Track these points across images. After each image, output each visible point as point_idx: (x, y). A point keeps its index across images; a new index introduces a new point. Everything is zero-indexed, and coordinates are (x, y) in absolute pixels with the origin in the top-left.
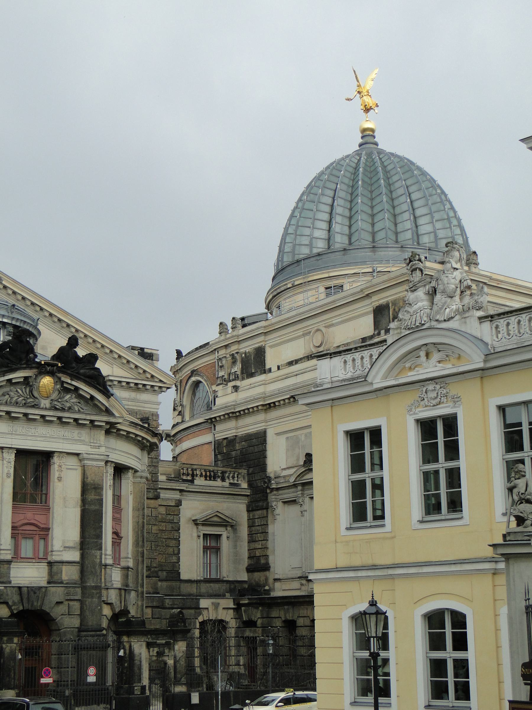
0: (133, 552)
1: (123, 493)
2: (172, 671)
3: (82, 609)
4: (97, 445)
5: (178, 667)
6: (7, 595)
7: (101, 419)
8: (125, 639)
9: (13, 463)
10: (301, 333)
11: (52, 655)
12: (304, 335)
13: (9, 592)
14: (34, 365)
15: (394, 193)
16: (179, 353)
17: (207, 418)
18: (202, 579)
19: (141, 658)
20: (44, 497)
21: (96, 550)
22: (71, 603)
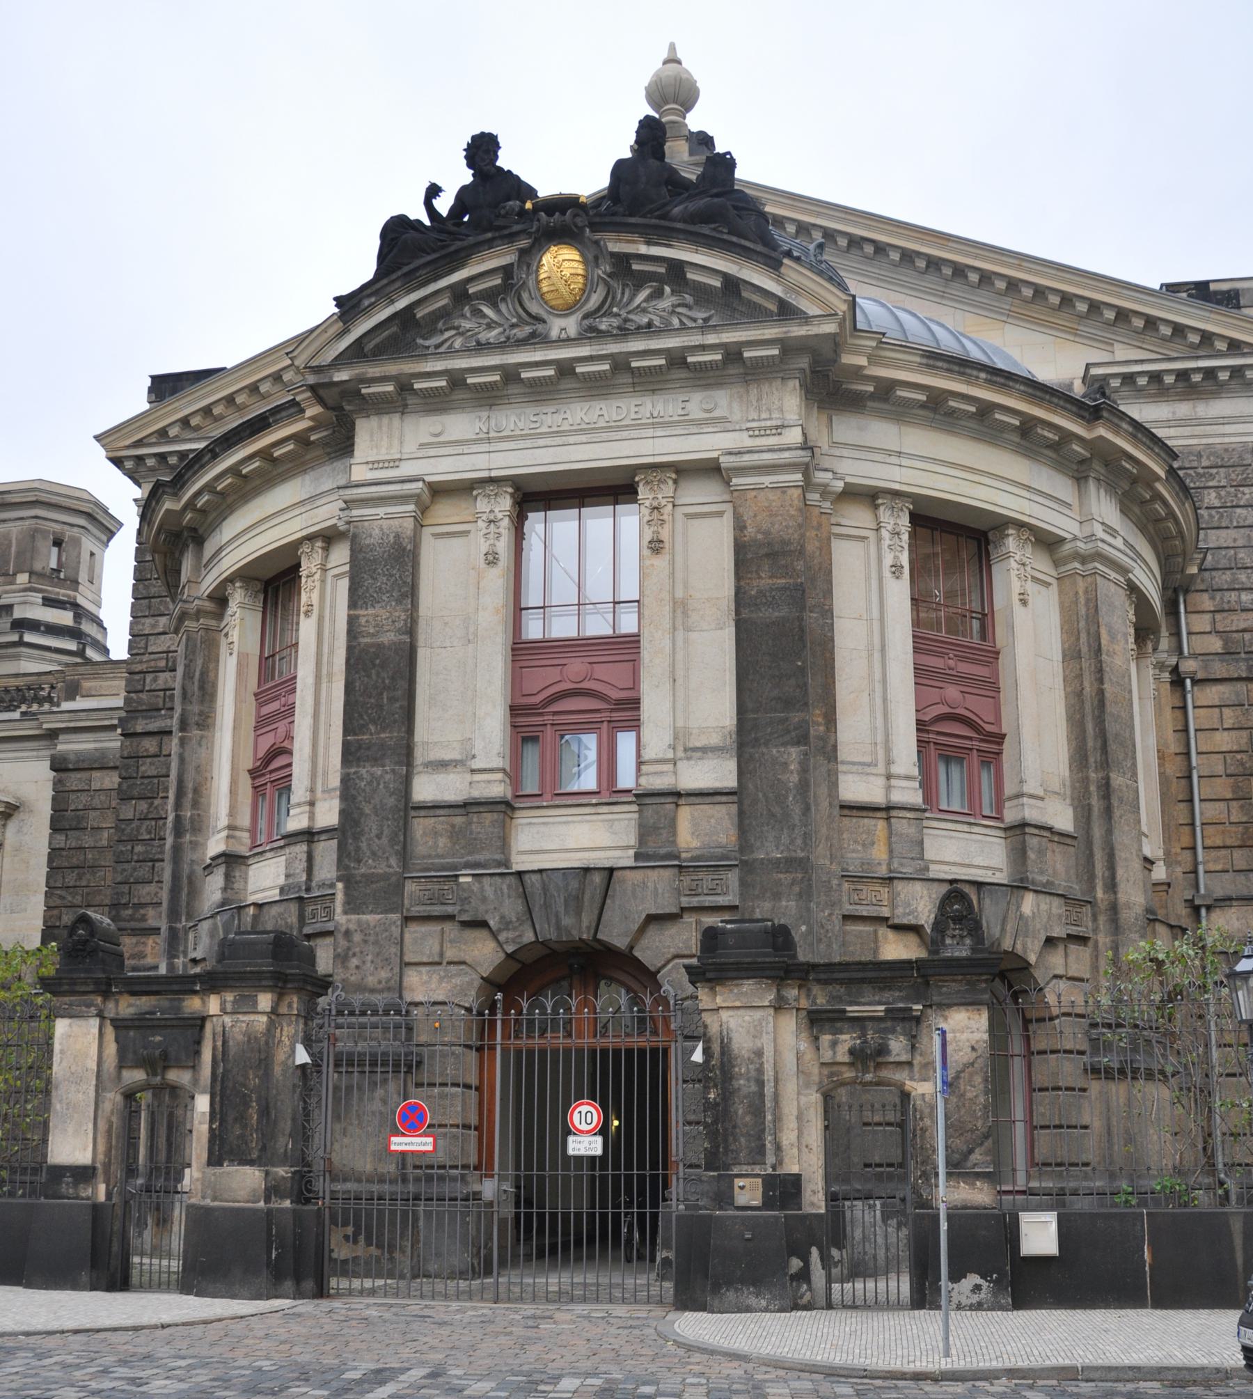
4: (769, 423)
6: (484, 900)
13: (489, 892)
19: (760, 1071)
21: (784, 744)
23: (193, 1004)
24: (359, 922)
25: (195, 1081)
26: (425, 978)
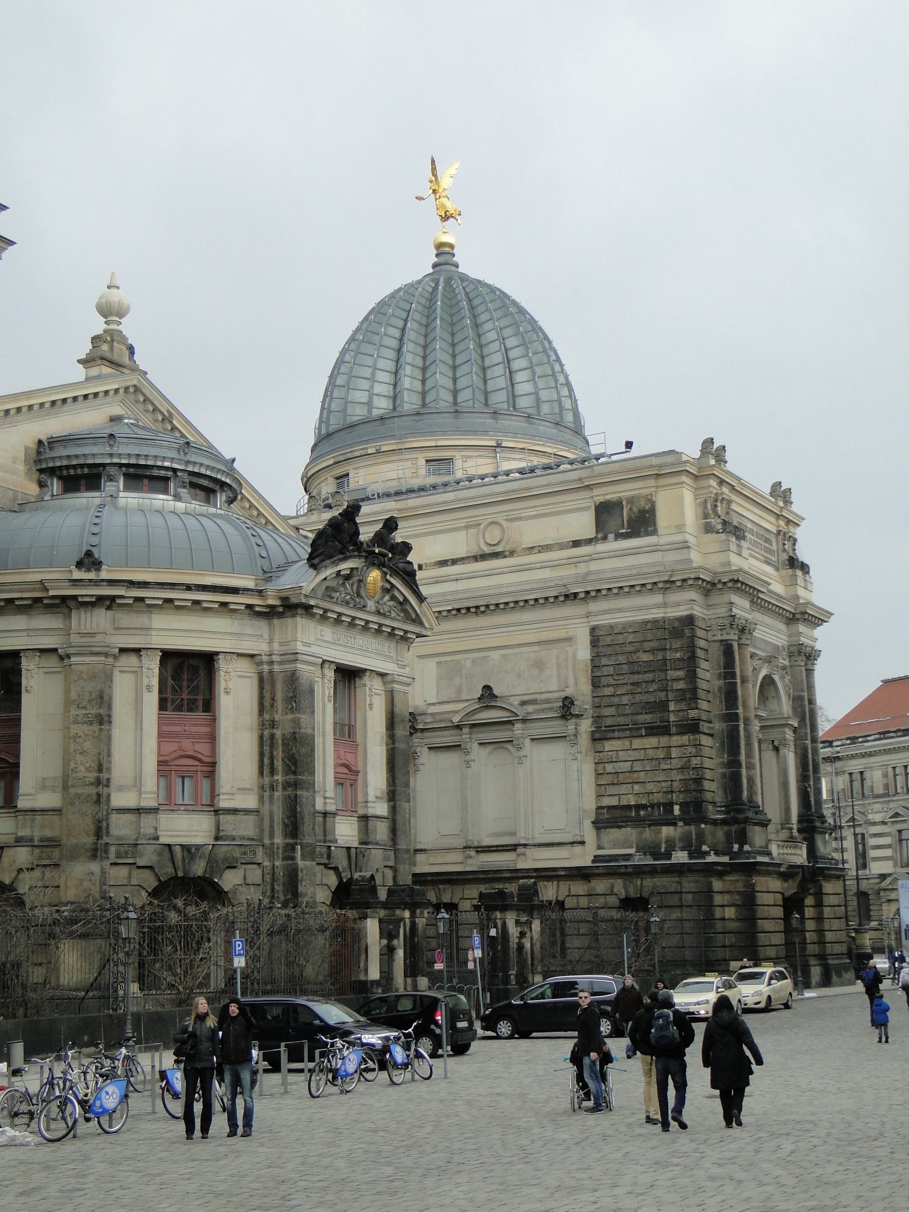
10: (463, 524)
12: (467, 527)
15: (483, 338)
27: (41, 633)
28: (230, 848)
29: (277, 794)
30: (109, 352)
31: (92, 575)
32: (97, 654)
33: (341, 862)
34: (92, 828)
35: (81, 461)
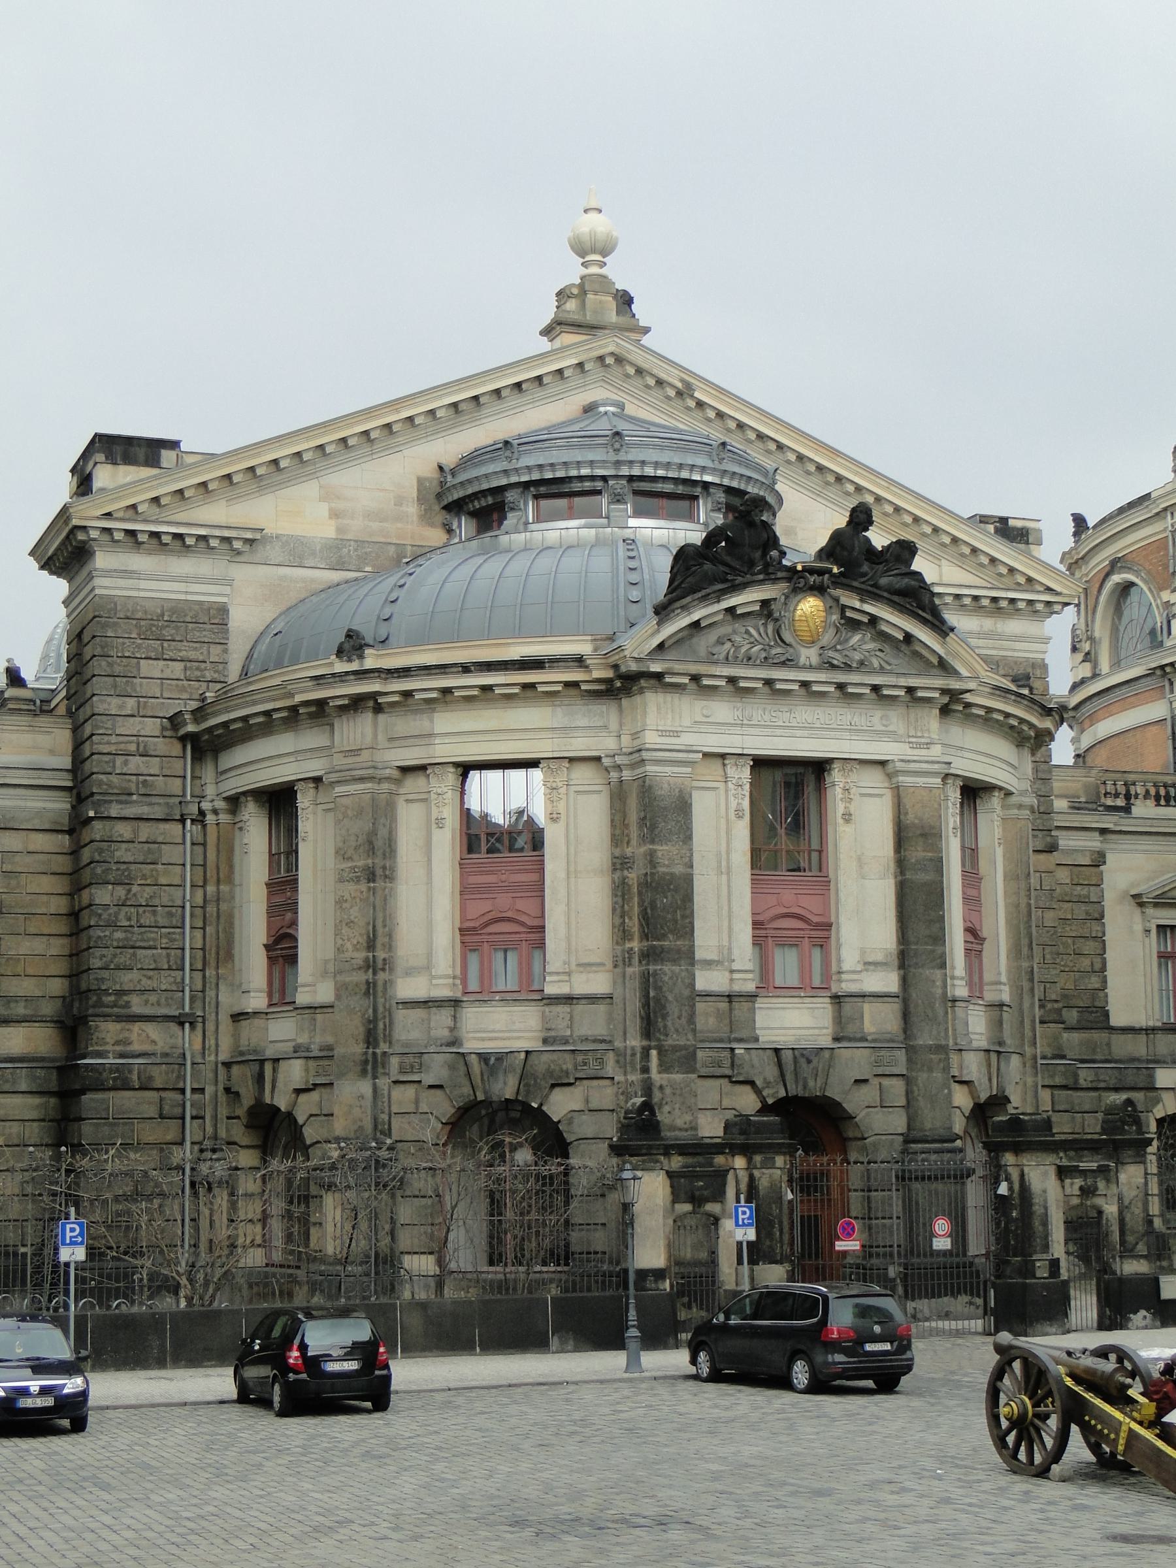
0: (1009, 971)
1: (982, 843)
2: (1115, 1229)
3: (908, 1093)
4: (923, 740)
5: (1127, 1219)
7: (930, 684)
8: (1009, 1158)
9: (747, 787)
11: (849, 1190)
13: (756, 1061)
14: (780, 575)
16: (1079, 522)
17: (1153, 665)
18: (1159, 1024)
19: (1046, 1201)
20: (815, 855)
21: (933, 968)
22: (886, 1082)
23: (719, 1160)
24: (669, 1080)
25: (724, 1210)
26: (710, 1119)
27: (308, 755)
28: (555, 1056)
29: (629, 970)
30: (594, 314)
31: (354, 666)
32: (362, 779)
33: (765, 1072)
34: (361, 1031)
35: (475, 488)
